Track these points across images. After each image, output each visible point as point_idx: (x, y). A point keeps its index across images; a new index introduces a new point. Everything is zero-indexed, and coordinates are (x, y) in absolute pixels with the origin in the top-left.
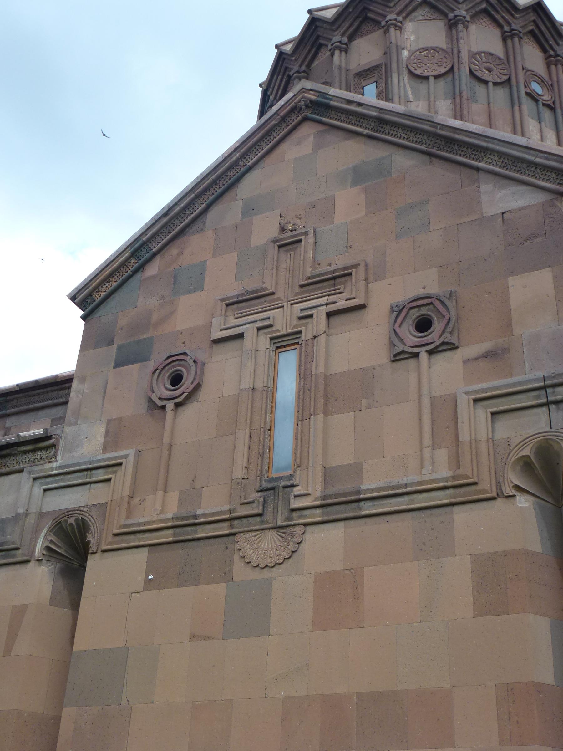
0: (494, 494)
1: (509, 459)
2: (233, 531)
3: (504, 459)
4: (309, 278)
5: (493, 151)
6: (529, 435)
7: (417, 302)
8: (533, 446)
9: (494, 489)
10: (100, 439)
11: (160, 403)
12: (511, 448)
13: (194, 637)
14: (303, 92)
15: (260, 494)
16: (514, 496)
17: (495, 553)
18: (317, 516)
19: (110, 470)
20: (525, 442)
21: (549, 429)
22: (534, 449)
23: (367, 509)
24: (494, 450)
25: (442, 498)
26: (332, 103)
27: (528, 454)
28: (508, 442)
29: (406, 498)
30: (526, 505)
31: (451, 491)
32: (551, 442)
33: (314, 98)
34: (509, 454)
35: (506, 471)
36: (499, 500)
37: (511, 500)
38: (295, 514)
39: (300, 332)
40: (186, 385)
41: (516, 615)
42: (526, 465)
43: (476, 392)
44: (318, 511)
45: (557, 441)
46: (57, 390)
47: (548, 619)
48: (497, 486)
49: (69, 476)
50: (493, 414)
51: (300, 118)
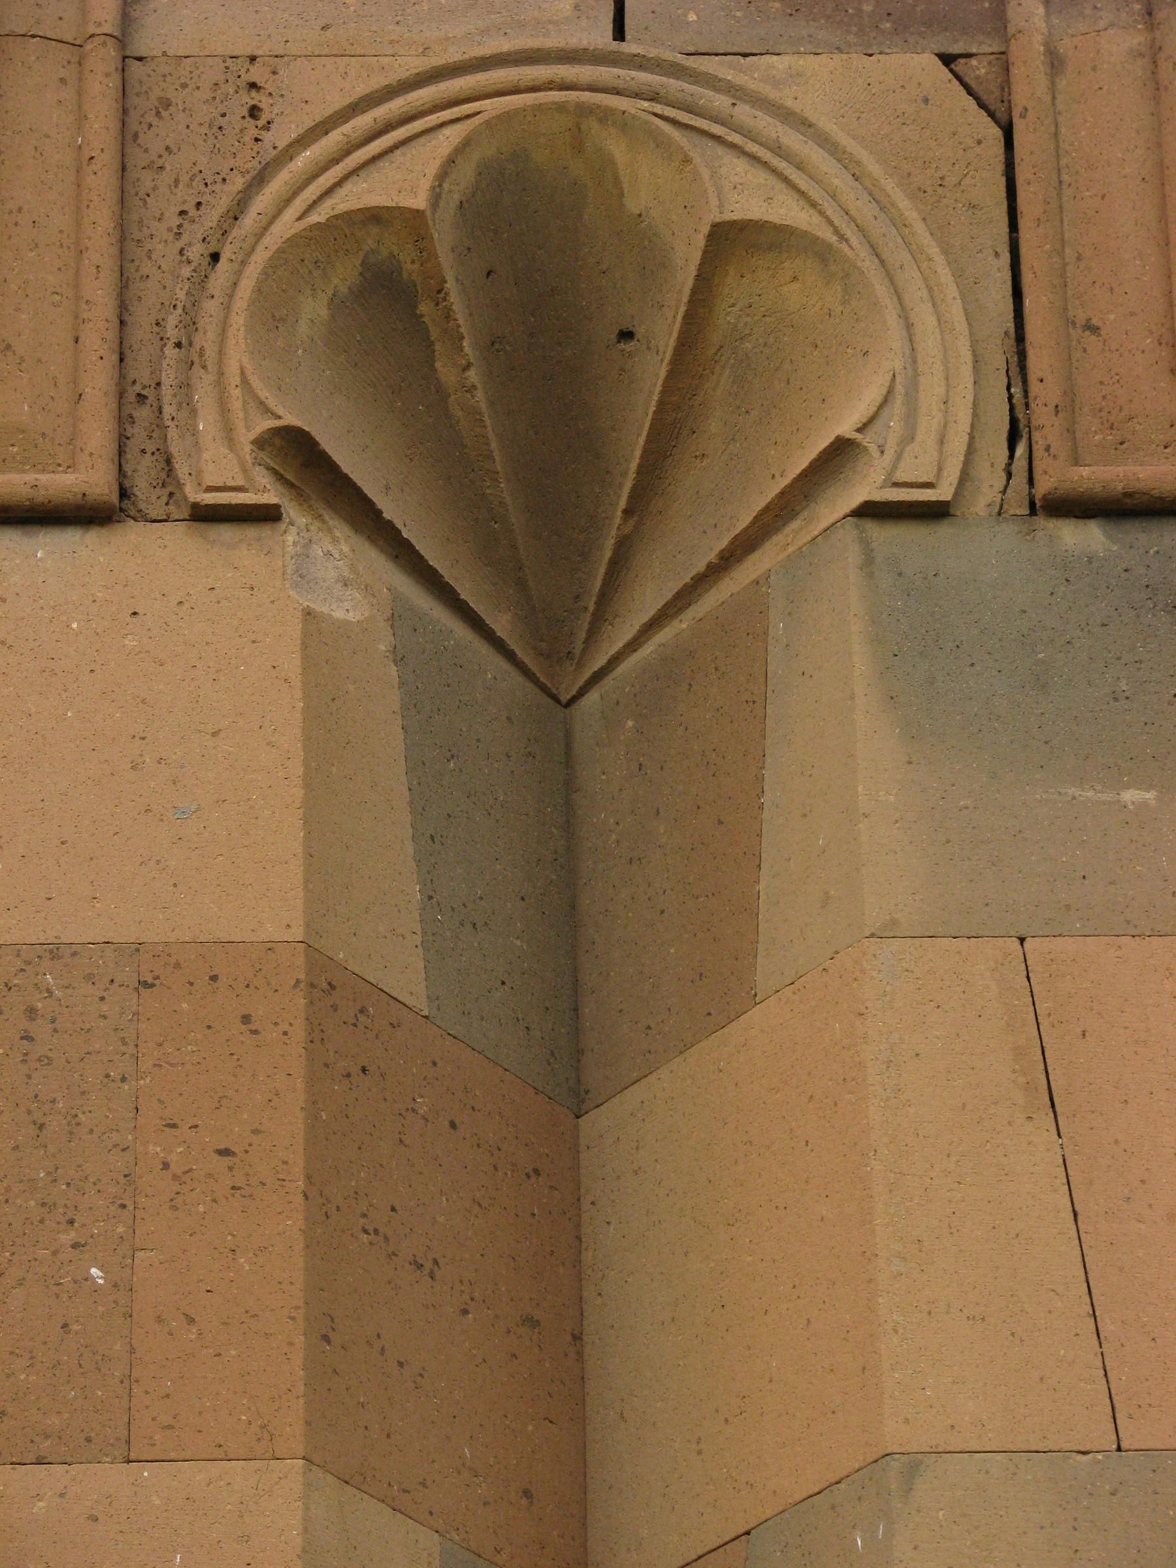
1: (249, 221)
3: (211, 218)
6: (436, 60)
8: (466, 144)
9: (98, 435)
12: (282, 135)
16: (267, 515)
17: (54, 951)
20: (397, 106)
21: (600, 36)
22: (466, 174)
24: (126, 136)
27: (420, 202)
28: (250, 88)
30: (346, 609)
32: (617, 149)
34: (260, 180)
35: (211, 307)
36: (131, 534)
37: (239, 545)
41: (197, 1475)
42: (380, 291)
45: (660, 143)
47: (429, 1541)
48: (123, 421)
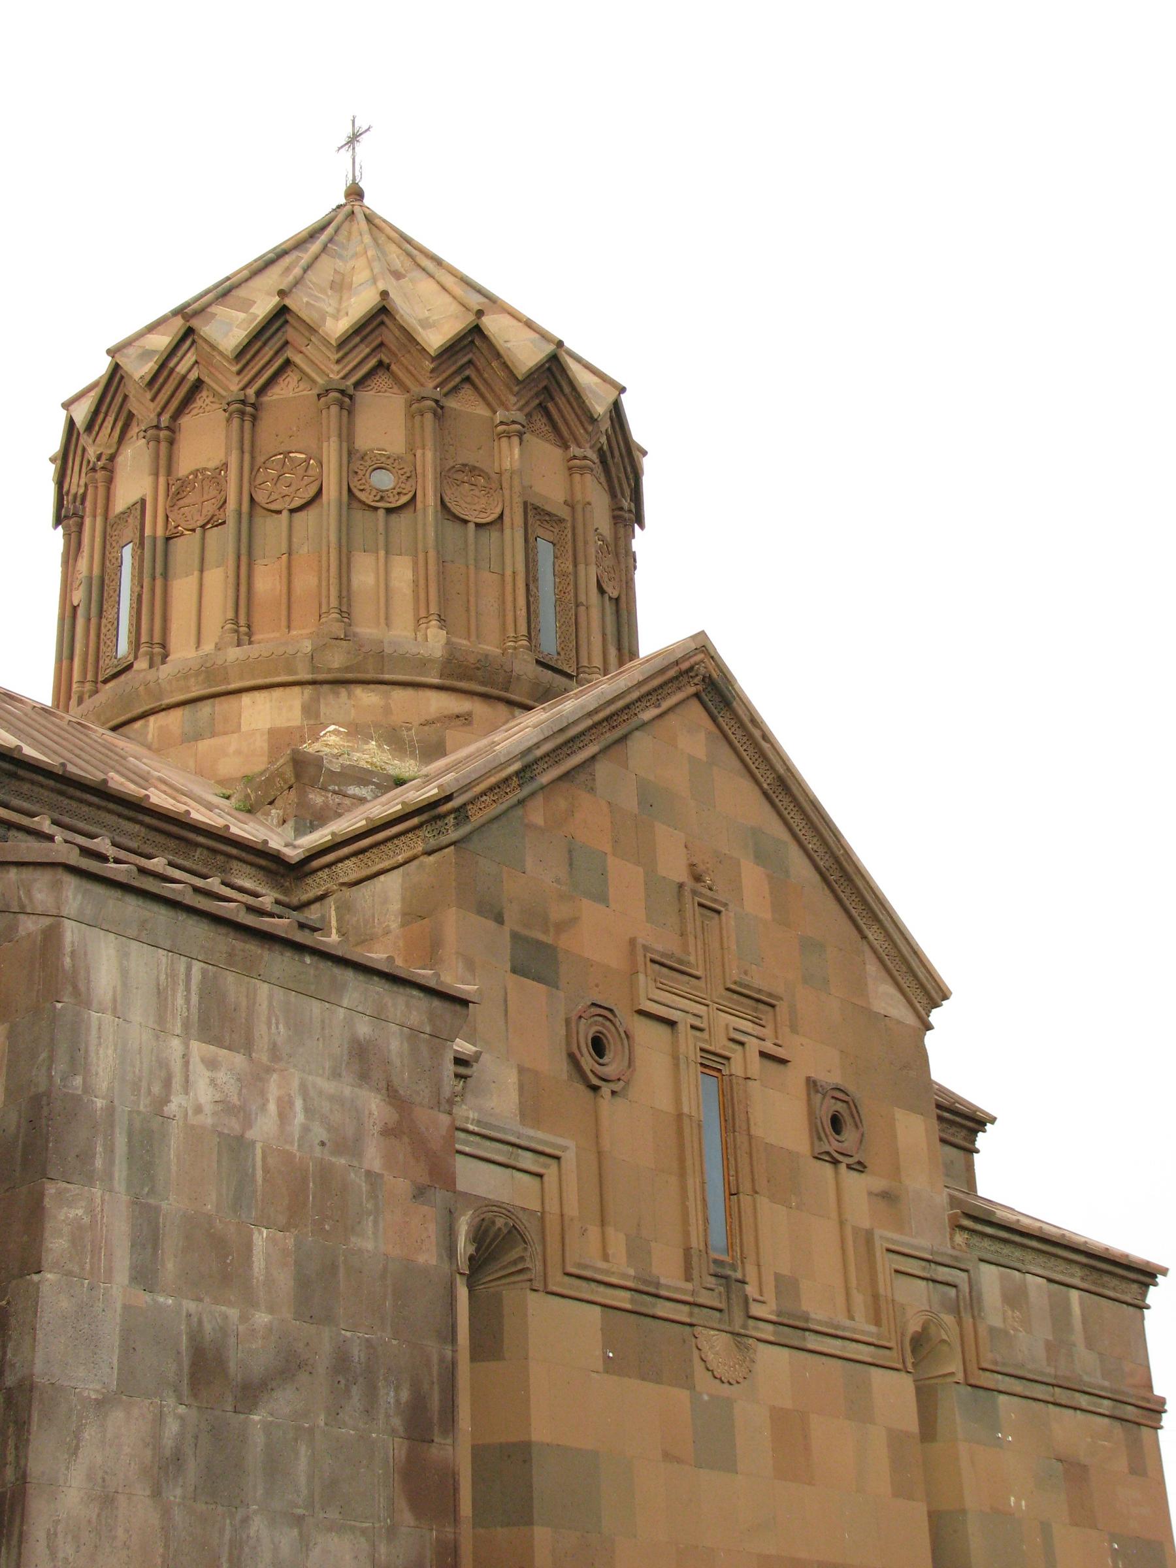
0: (900, 1366)
2: (694, 1321)
4: (735, 983)
5: (882, 926)
7: (839, 1093)
10: (514, 1096)
11: (595, 1081)
13: (667, 1456)
14: (703, 652)
15: (713, 1280)
18: (767, 1331)
19: (542, 1159)
23: (813, 1342)
25: (864, 1353)
26: (735, 704)
29: (839, 1342)
31: (872, 1348)
33: (715, 675)
38: (751, 1322)
39: (728, 1059)
40: (612, 1066)
43: (888, 1240)
44: (770, 1327)
46: (120, 815)
49: (488, 1143)
50: (897, 1271)
51: (692, 690)
